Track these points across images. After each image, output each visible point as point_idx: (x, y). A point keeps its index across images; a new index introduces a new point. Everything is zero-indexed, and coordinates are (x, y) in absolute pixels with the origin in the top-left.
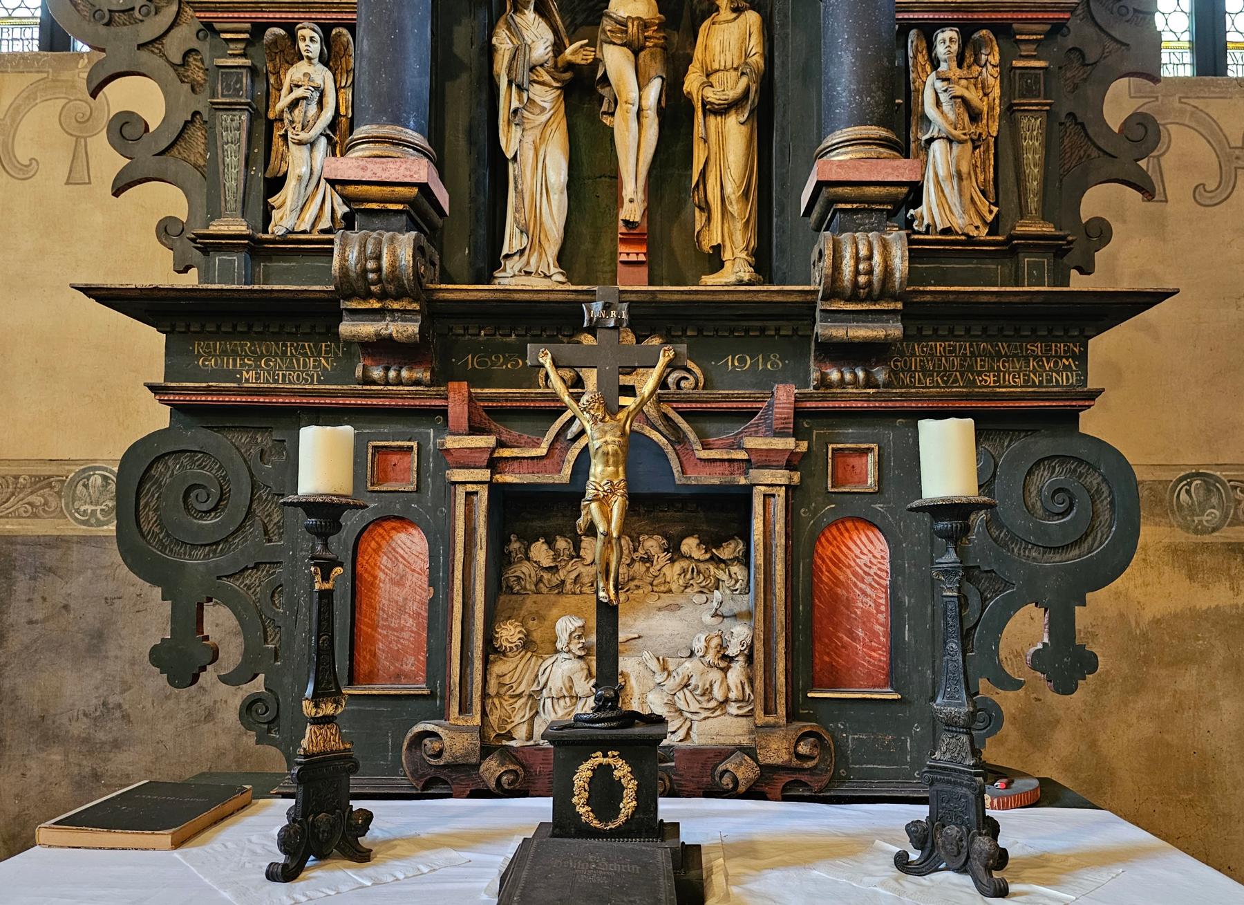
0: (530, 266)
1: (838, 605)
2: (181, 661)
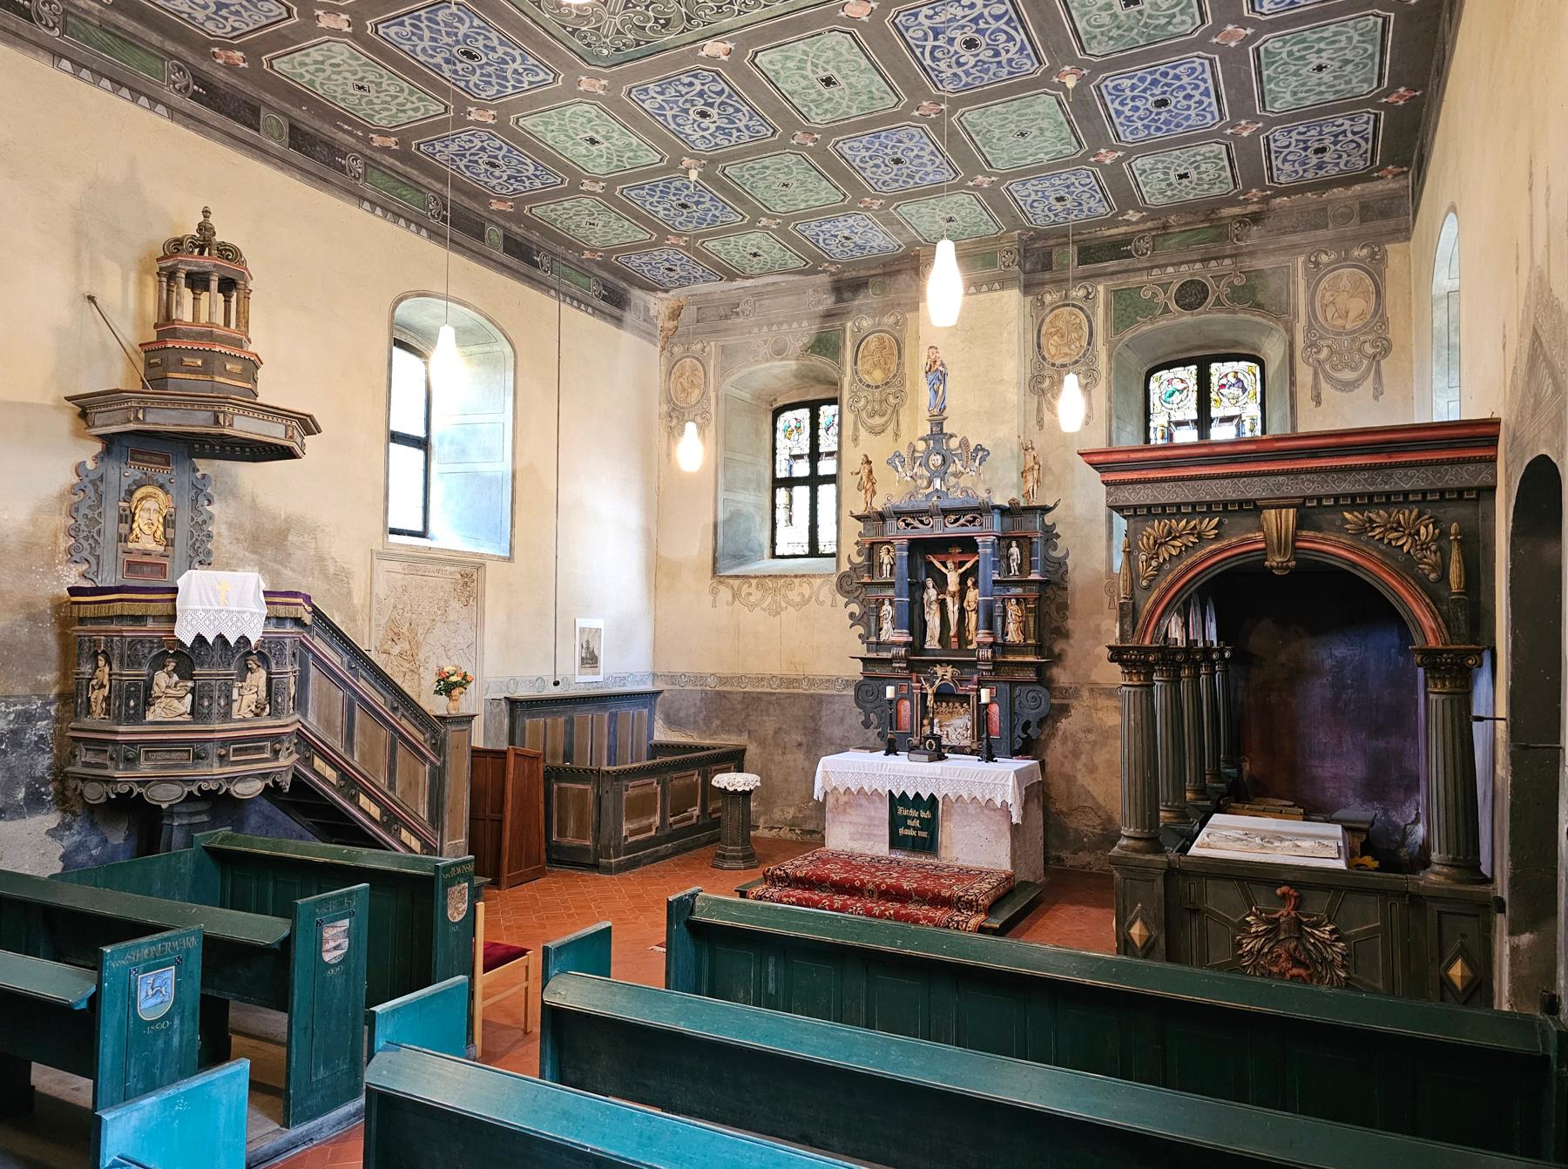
0: (932, 643)
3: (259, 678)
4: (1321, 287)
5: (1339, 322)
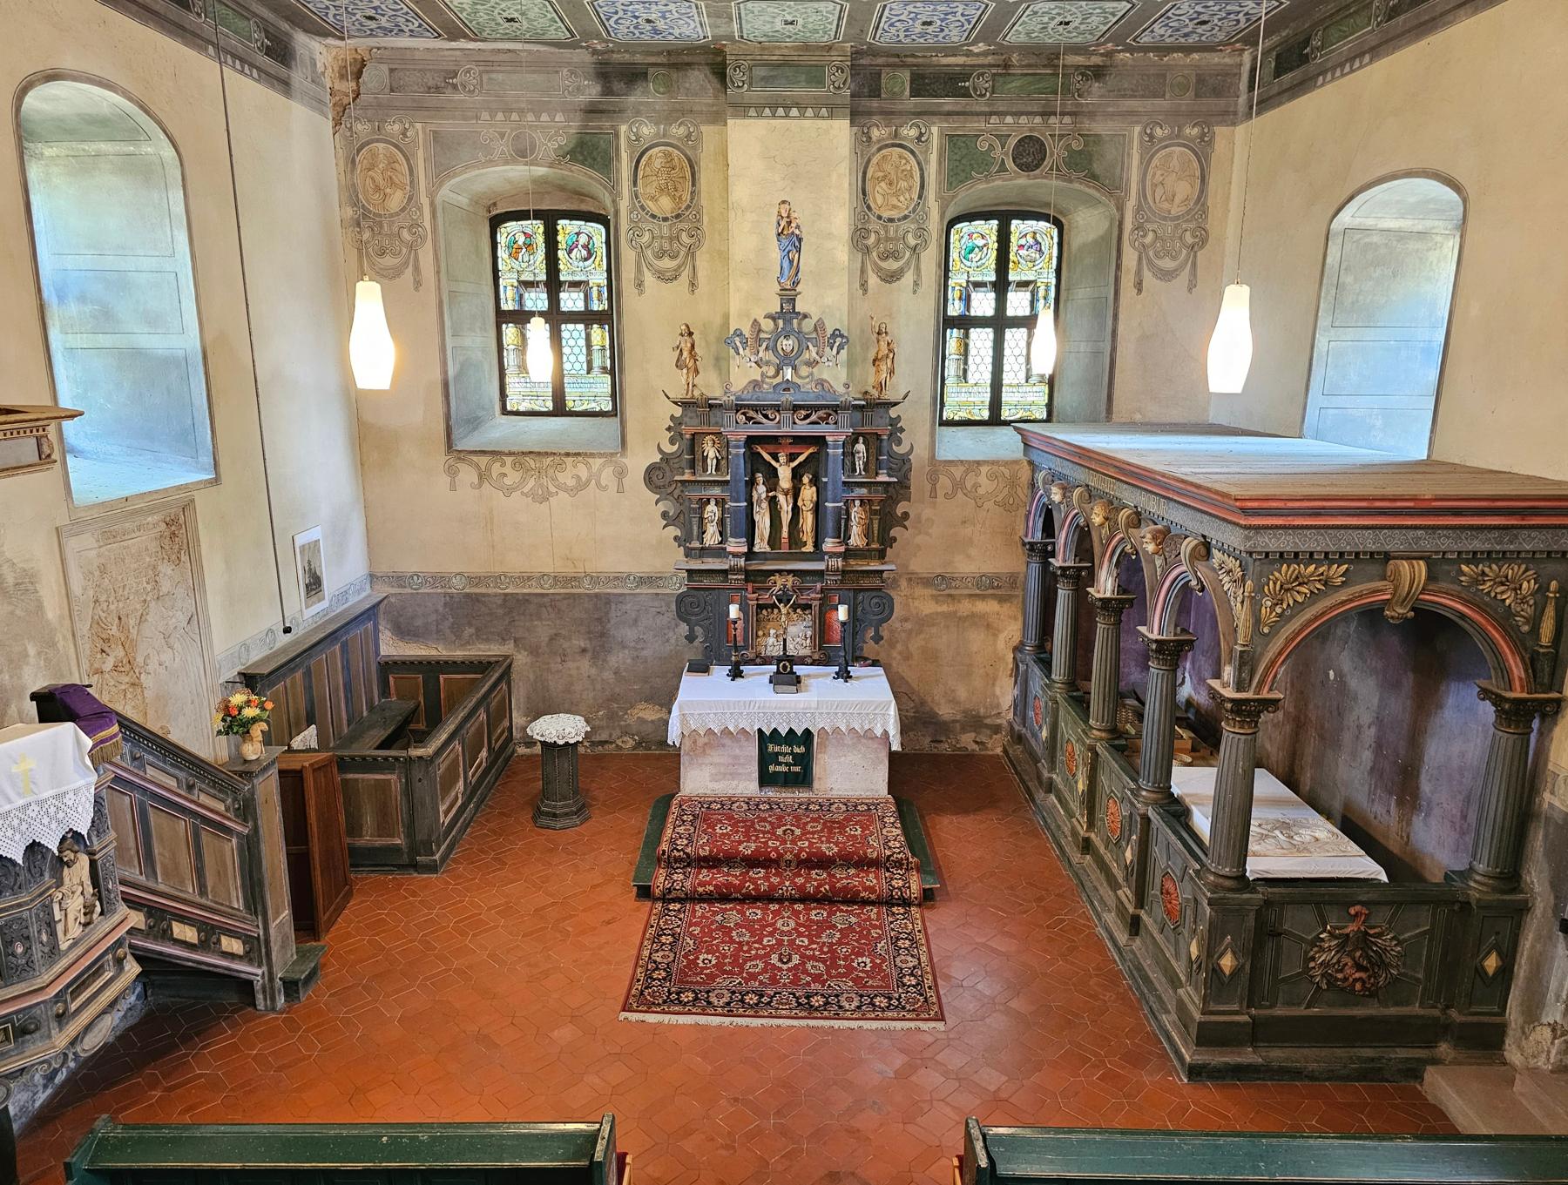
0: (761, 545)
1: (830, 627)
2: (691, 638)
3: (80, 870)
4: (1153, 164)
5: (1166, 206)
